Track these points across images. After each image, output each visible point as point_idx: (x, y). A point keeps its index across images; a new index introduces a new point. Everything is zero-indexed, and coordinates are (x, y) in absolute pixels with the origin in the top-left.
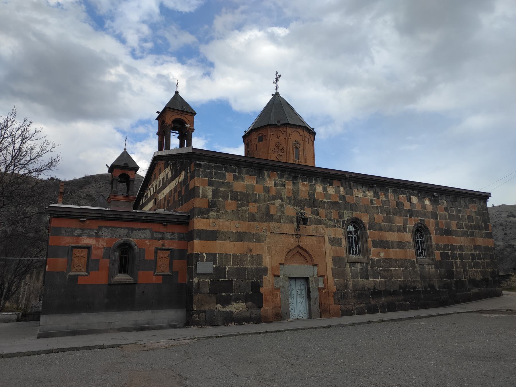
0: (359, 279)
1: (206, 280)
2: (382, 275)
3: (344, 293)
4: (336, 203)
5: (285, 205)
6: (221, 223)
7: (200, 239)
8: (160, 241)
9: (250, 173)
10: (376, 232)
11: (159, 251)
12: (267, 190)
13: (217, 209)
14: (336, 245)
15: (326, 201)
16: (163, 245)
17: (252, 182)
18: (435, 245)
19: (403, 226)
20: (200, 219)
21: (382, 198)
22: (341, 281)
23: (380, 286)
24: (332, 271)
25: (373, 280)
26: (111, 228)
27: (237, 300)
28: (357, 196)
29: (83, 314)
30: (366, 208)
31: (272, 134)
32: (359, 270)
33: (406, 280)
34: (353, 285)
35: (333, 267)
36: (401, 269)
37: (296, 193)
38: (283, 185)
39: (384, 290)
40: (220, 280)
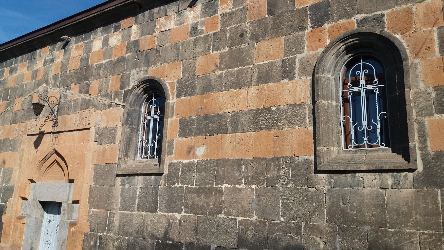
0: (136, 210)
2: (190, 203)
3: (102, 238)
5: (49, 90)
10: (194, 98)
14: (106, 142)
15: (104, 62)
18: (434, 95)
19: (280, 64)
22: (100, 212)
23: (180, 231)
24: (90, 192)
25: (165, 216)
28: (163, 30)
30: (179, 49)
32: (139, 191)
33: (265, 223)
34: (119, 222)
35: (92, 184)
36: (254, 187)
39: (189, 243)
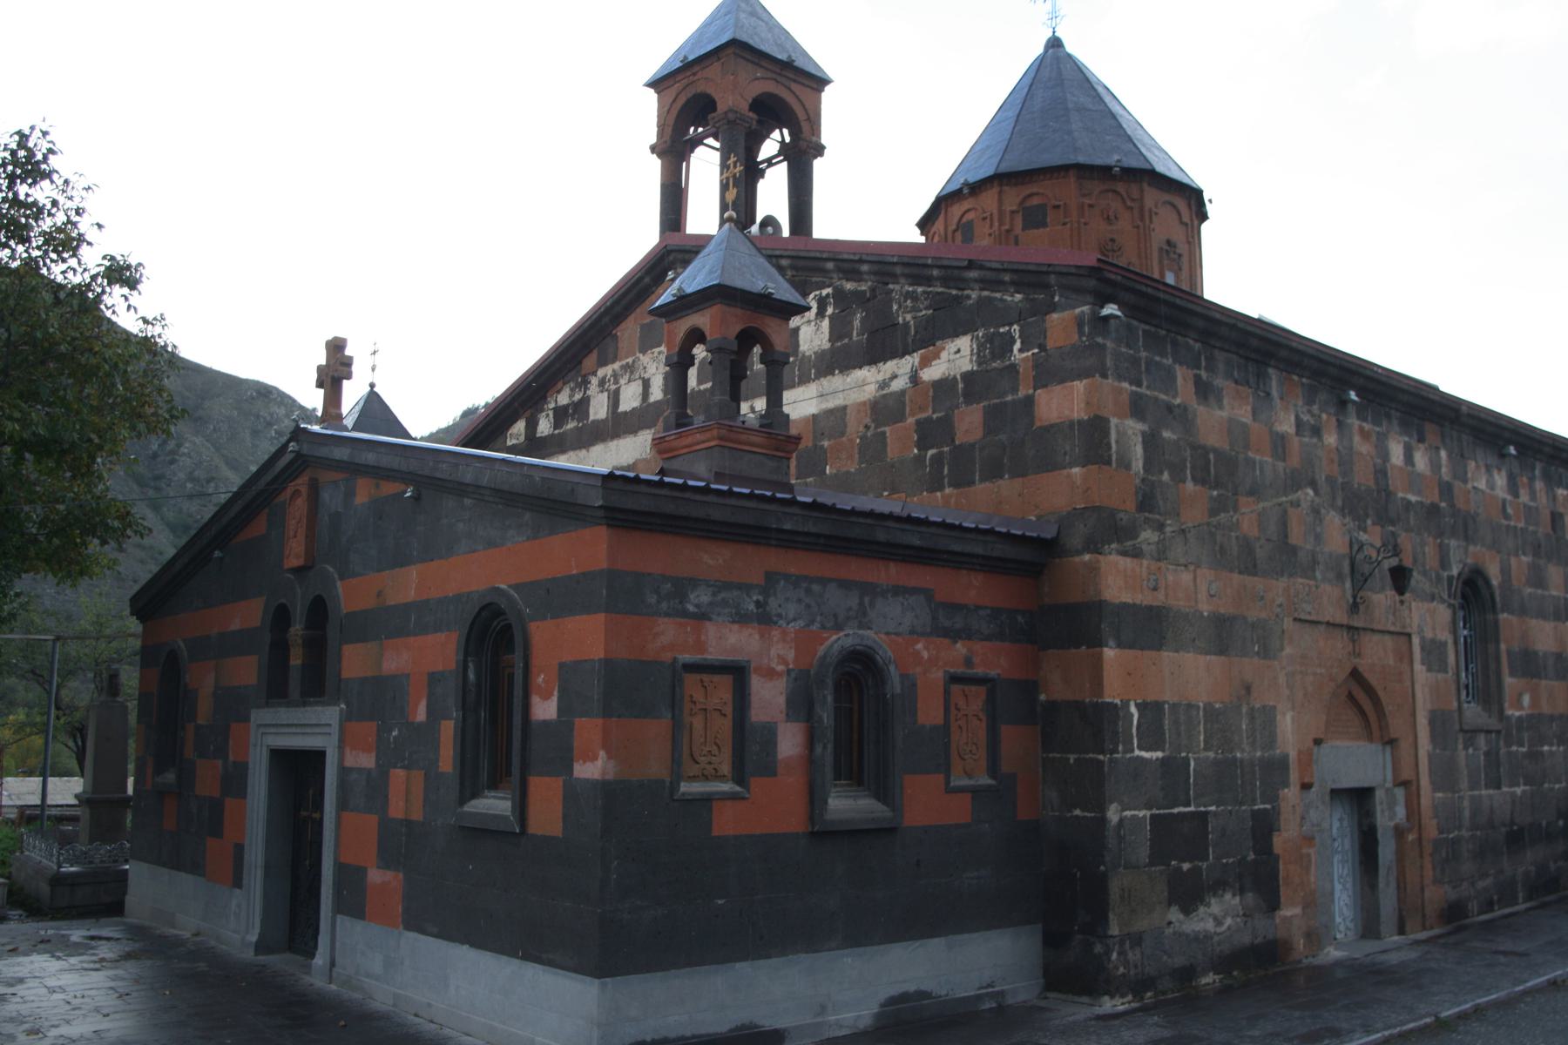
0: (1483, 787)
1: (1141, 814)
4: (1432, 511)
5: (1323, 511)
6: (1170, 578)
7: (1119, 646)
8: (959, 645)
9: (1236, 373)
11: (955, 688)
12: (1279, 444)
13: (1158, 517)
15: (1413, 498)
16: (968, 662)
17: (1243, 412)
20: (1114, 558)
21: (1524, 497)
26: (804, 585)
27: (1218, 886)
29: (738, 965)
31: (1091, 206)
32: (1482, 758)
35: (1430, 748)
37: (1345, 459)
38: (1317, 431)
40: (1176, 810)
